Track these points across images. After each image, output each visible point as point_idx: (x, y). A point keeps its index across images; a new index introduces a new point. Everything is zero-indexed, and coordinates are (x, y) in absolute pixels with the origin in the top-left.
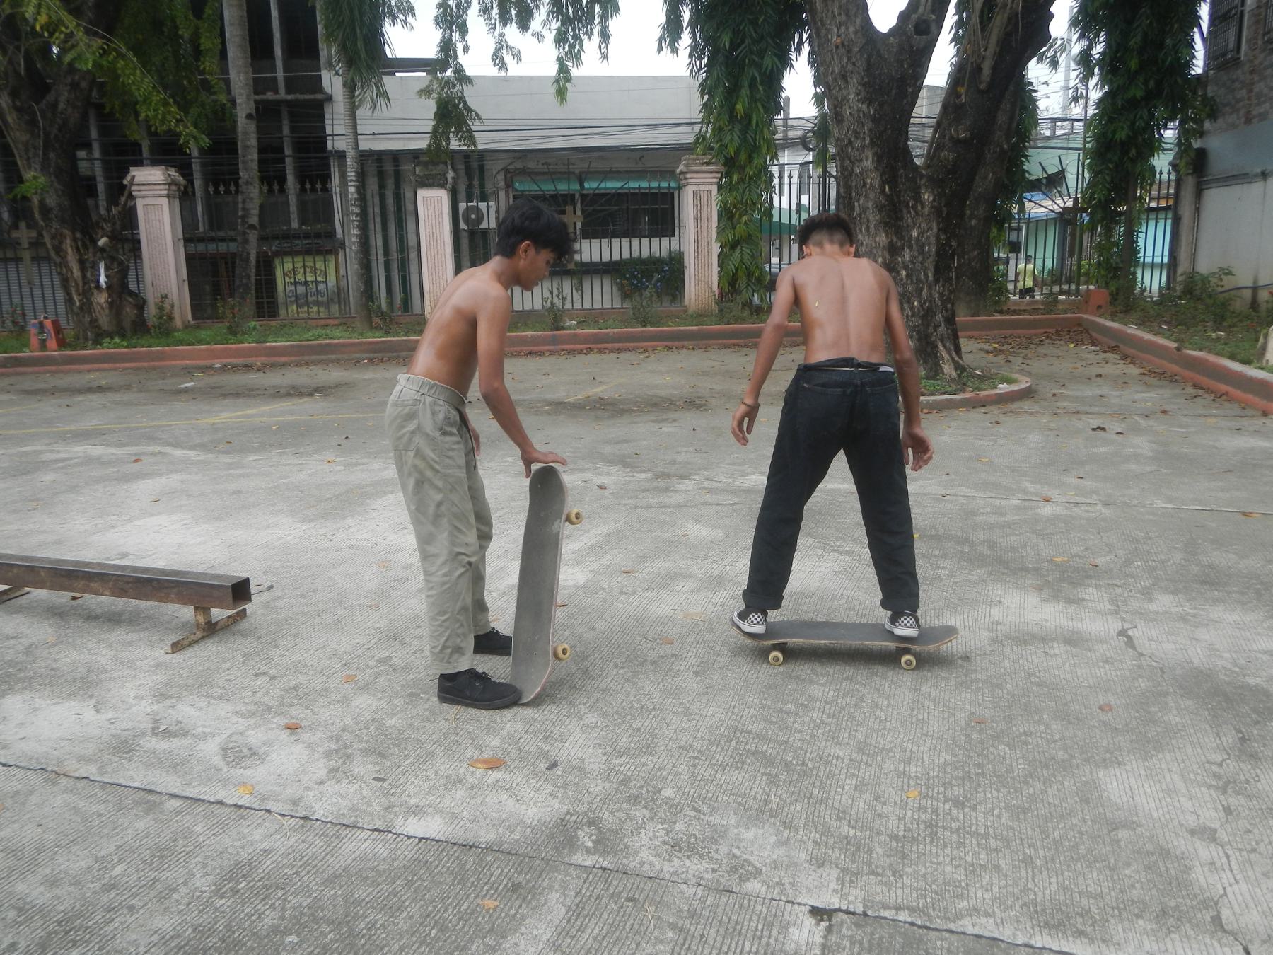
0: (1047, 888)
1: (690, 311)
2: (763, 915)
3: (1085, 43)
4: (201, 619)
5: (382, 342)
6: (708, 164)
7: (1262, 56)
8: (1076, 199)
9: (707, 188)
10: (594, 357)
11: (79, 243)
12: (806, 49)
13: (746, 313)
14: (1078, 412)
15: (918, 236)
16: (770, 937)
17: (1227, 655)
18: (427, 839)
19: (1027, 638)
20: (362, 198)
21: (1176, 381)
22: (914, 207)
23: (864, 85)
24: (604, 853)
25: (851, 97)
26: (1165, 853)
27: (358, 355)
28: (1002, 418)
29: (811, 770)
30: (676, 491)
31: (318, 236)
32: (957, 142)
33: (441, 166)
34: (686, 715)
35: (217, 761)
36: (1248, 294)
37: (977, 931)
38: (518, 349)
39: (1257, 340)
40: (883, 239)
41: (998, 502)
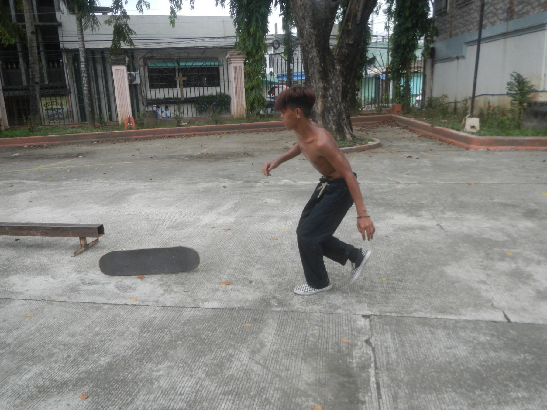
0: (437, 302)
1: (234, 118)
2: (346, 319)
3: (389, 4)
4: (83, 243)
5: (103, 133)
6: (239, 54)
7: (455, 11)
8: (387, 69)
9: (239, 65)
10: (197, 138)
12: (279, 6)
13: (258, 118)
14: (399, 152)
15: (335, 84)
16: (351, 325)
17: (475, 229)
18: (215, 308)
19: (406, 229)
20: (87, 70)
21: (432, 139)
22: (333, 72)
23: (312, 21)
24: (283, 306)
25: (307, 26)
26: (472, 289)
28: (372, 155)
29: (346, 275)
30: (256, 187)
31: (57, 88)
32: (348, 45)
34: (293, 262)
35: (116, 291)
36: (453, 105)
37: (419, 316)
38: (162, 135)
39: (461, 121)
40: (321, 85)
41: (380, 185)
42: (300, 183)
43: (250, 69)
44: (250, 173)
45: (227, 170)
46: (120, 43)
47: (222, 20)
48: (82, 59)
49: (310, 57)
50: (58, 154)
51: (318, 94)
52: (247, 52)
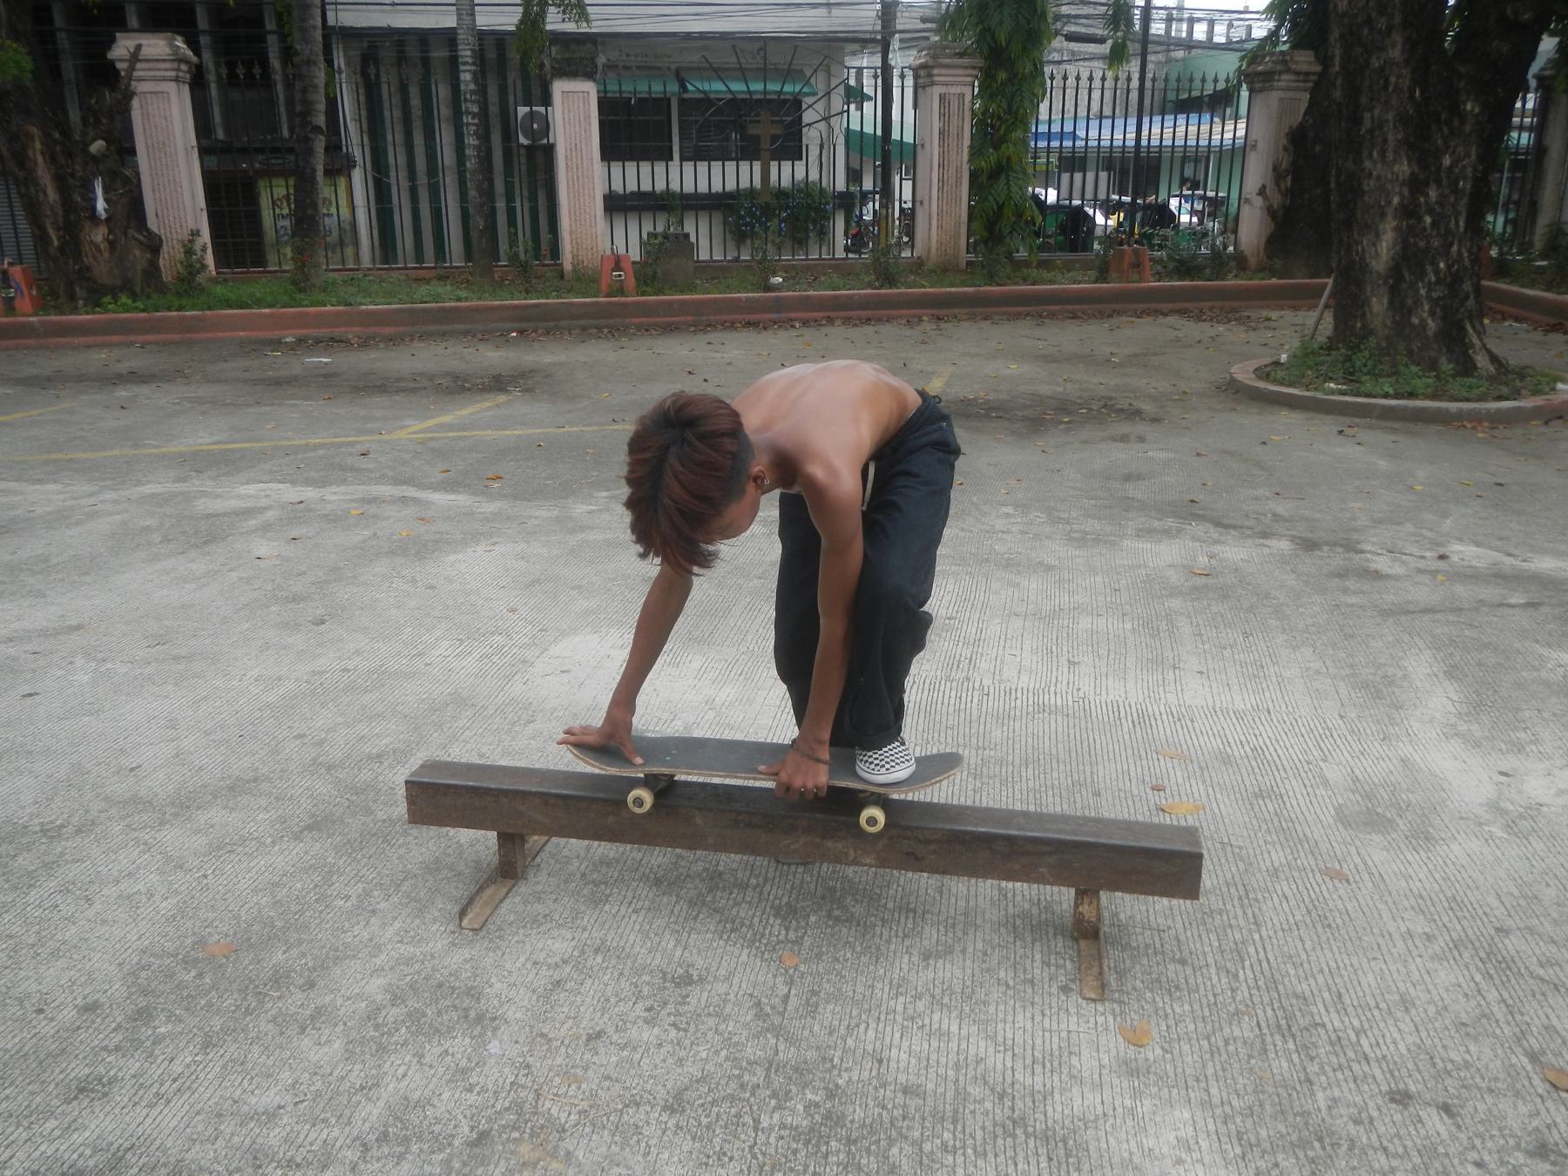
6: (961, 55)
11: (58, 148)
20: (482, 91)
30: (1388, 577)
33: (589, 45)
40: (1404, 168)
42: (1546, 564)
44: (1257, 499)
46: (542, 15)
48: (466, 53)
49: (1375, 64)
50: (421, 374)
51: (1389, 203)
52: (990, 46)
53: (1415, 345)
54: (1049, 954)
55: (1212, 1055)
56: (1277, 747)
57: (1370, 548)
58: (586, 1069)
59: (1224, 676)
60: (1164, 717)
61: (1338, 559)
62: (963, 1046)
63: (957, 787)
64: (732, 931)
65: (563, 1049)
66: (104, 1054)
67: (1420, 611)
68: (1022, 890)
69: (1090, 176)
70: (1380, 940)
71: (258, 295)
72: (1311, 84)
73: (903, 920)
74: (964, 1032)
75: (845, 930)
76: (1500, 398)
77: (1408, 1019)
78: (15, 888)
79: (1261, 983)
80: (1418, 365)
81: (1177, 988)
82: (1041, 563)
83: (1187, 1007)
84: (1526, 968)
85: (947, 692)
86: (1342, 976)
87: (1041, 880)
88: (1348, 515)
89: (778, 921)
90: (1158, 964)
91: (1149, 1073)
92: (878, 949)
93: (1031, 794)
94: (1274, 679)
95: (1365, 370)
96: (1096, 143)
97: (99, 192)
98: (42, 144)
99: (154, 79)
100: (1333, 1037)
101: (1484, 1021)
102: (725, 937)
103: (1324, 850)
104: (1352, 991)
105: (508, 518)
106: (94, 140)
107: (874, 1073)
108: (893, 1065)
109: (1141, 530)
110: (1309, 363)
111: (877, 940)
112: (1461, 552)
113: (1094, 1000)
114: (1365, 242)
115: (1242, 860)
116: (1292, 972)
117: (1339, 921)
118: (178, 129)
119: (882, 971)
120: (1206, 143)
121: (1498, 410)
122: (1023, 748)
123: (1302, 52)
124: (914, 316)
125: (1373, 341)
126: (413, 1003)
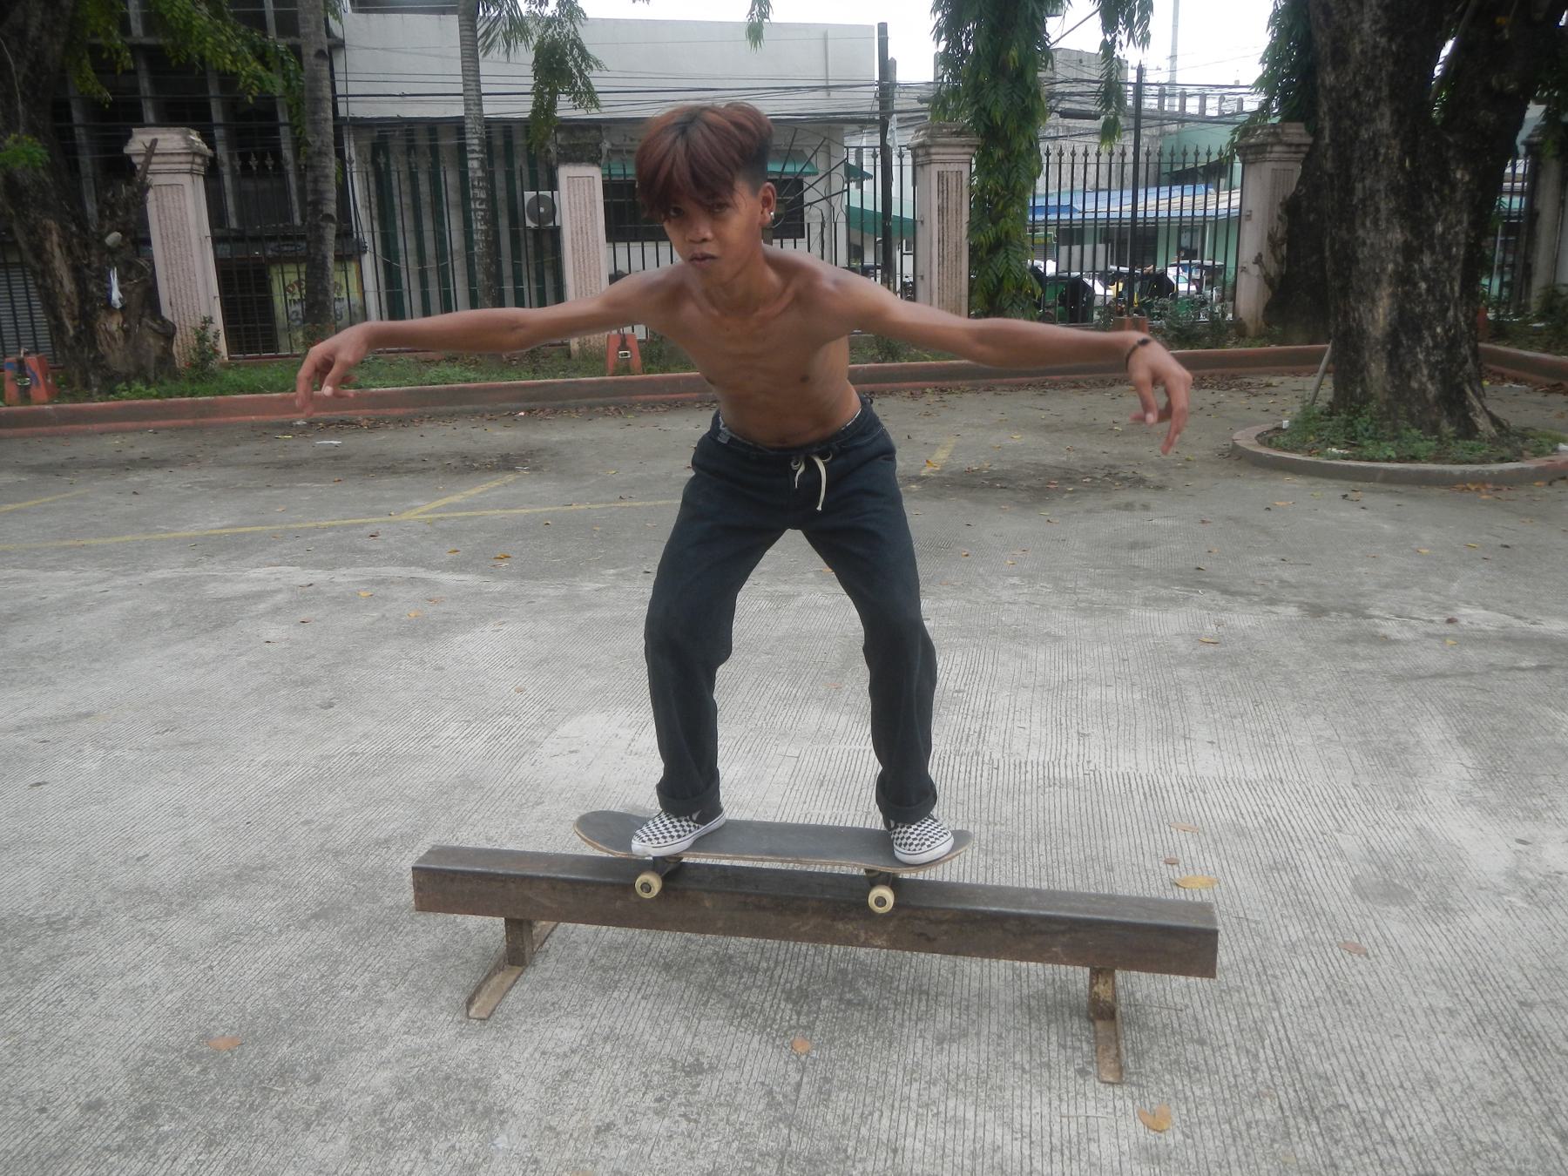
6: (958, 134)
15: (1444, 233)
20: (490, 177)
25: (1366, 26)
27: (508, 405)
30: (1396, 642)
33: (594, 132)
40: (1397, 236)
42: (1555, 626)
43: (990, 184)
44: (1263, 565)
45: (1145, 545)
47: (824, 36)
48: (473, 142)
49: (1365, 135)
50: (430, 455)
51: (1383, 270)
53: (1416, 409)
54: (1065, 1035)
55: (1234, 1140)
56: (1291, 817)
57: (1377, 613)
58: (595, 1163)
59: (1235, 746)
60: (1176, 788)
61: (1346, 625)
62: (980, 1133)
63: (968, 864)
64: (743, 1016)
65: (572, 1143)
66: (107, 1154)
67: (1431, 676)
68: (1036, 971)
69: (1088, 248)
70: (1402, 1016)
71: (270, 379)
72: (1303, 156)
73: (916, 1002)
74: (980, 1119)
75: (857, 1014)
76: (1502, 460)
77: (1433, 1099)
78: (19, 982)
79: (1282, 1063)
80: (1420, 428)
81: (1197, 1069)
82: (1048, 634)
83: (1207, 1090)
84: (1552, 1043)
85: (957, 767)
86: (1363, 1053)
87: (1055, 960)
88: (1355, 580)
89: (790, 1006)
90: (1176, 1044)
91: (1170, 1159)
92: (891, 1033)
93: (1043, 871)
94: (1286, 748)
95: (1367, 434)
96: (1093, 216)
97: (115, 282)
98: (59, 236)
99: (170, 172)
100: (1358, 1119)
101: (1511, 1099)
102: (736, 1023)
103: (1341, 924)
104: (1375, 1071)
105: (517, 597)
106: (109, 232)
107: (889, 1163)
108: (908, 1154)
109: (1147, 599)
110: (1310, 428)
111: (890, 1023)
112: (1470, 615)
113: (1112, 1084)
114: (1361, 309)
115: (1259, 935)
116: (1313, 1051)
117: (1360, 997)
118: (192, 218)
119: (895, 1057)
120: (1202, 213)
121: (1501, 472)
122: (1035, 823)
123: (1295, 124)
124: (916, 388)
125: (1373, 405)
126: (419, 1097)
